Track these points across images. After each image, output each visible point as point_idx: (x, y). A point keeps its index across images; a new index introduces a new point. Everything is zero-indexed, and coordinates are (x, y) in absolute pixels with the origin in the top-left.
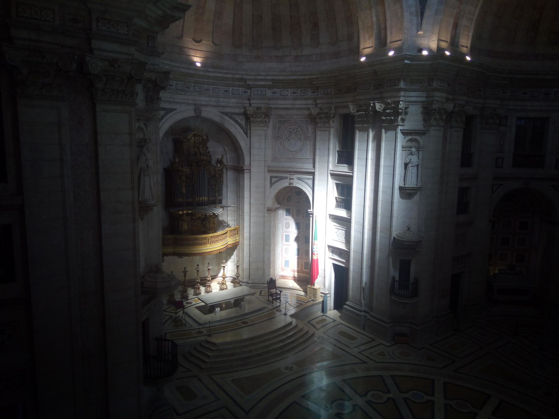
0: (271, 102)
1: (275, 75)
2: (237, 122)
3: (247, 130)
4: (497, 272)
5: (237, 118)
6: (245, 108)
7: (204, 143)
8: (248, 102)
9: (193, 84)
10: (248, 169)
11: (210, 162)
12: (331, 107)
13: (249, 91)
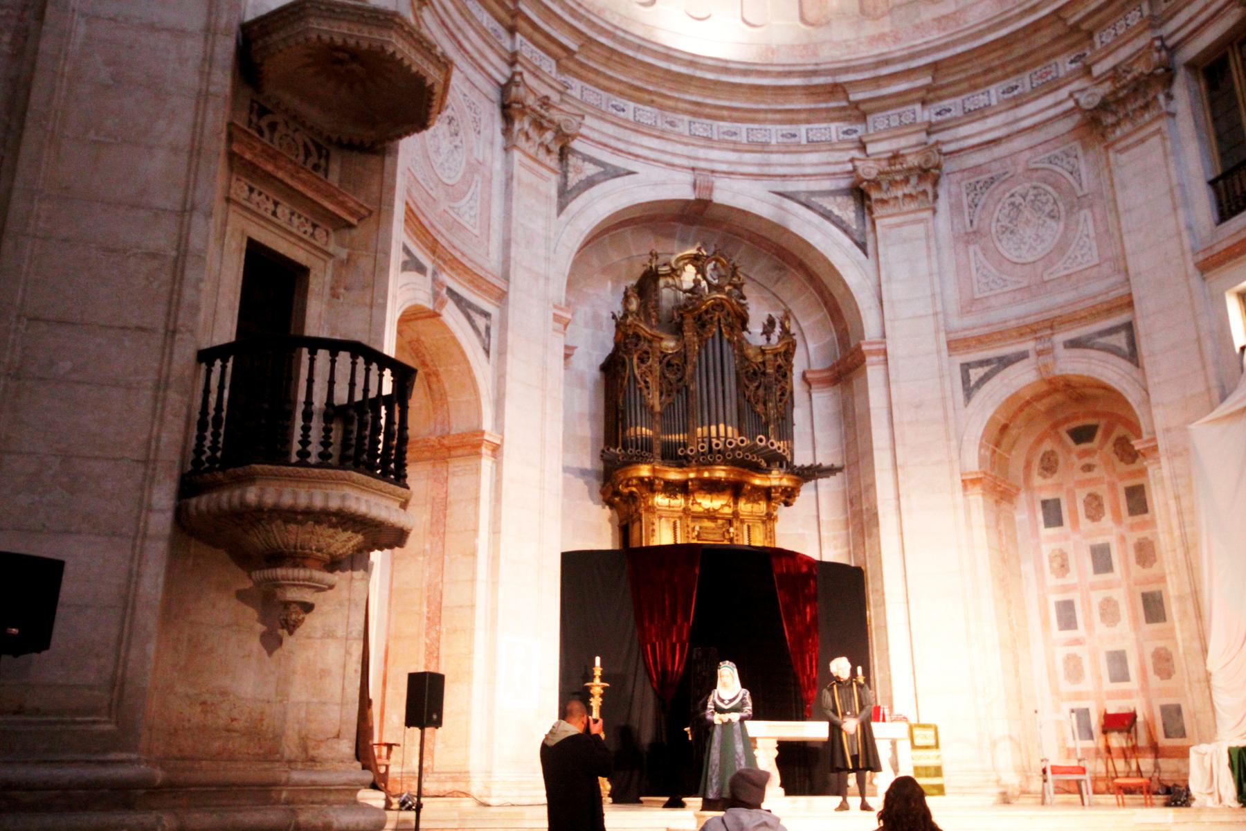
0: (934, 138)
2: (827, 215)
3: (863, 234)
9: (687, 118)
10: (877, 353)
11: (743, 321)
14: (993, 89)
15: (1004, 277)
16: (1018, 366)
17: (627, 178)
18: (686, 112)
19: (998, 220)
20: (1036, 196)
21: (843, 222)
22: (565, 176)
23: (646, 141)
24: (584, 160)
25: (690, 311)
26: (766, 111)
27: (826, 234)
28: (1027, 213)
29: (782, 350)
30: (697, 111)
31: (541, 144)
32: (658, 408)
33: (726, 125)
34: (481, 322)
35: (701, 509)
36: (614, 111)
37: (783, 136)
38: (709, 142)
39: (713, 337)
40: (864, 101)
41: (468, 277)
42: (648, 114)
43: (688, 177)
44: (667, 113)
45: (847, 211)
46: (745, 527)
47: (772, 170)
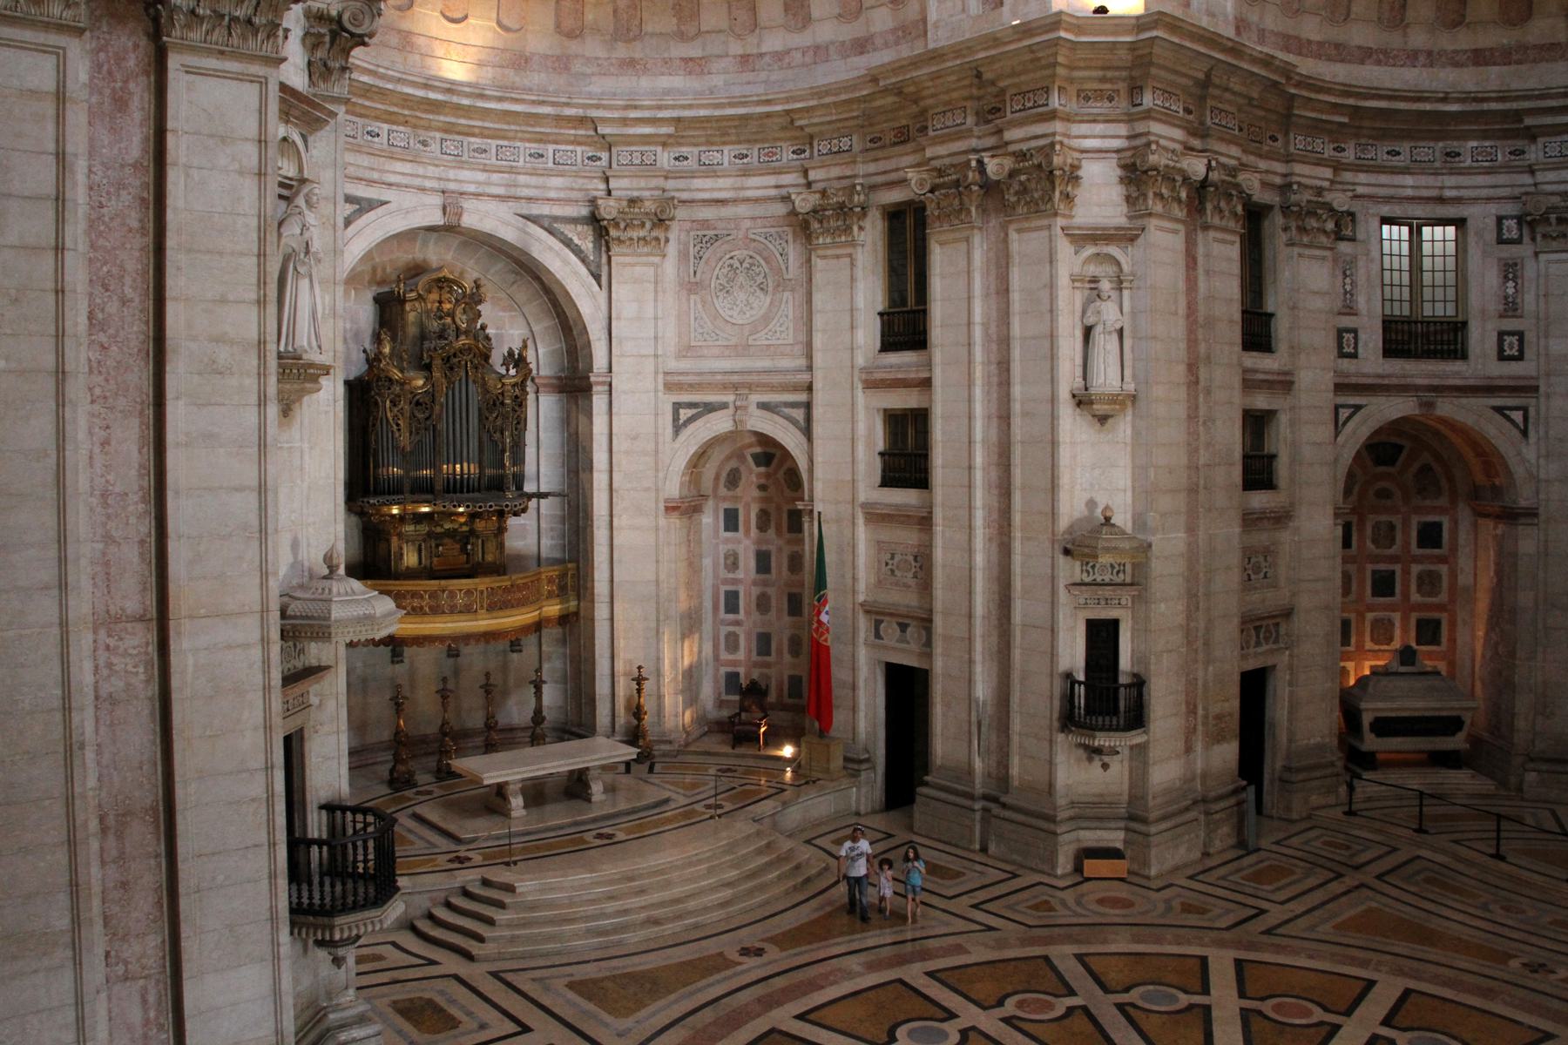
0: (671, 184)
1: (683, 107)
2: (568, 243)
3: (599, 266)
4: (1367, 672)
6: (593, 202)
7: (473, 300)
8: (602, 186)
9: (438, 135)
12: (854, 186)
13: (604, 155)
14: (726, 149)
18: (438, 130)
23: (399, 166)
27: (566, 262)
28: (741, 278)
30: (448, 129)
33: (476, 142)
42: (401, 134)
44: (420, 132)
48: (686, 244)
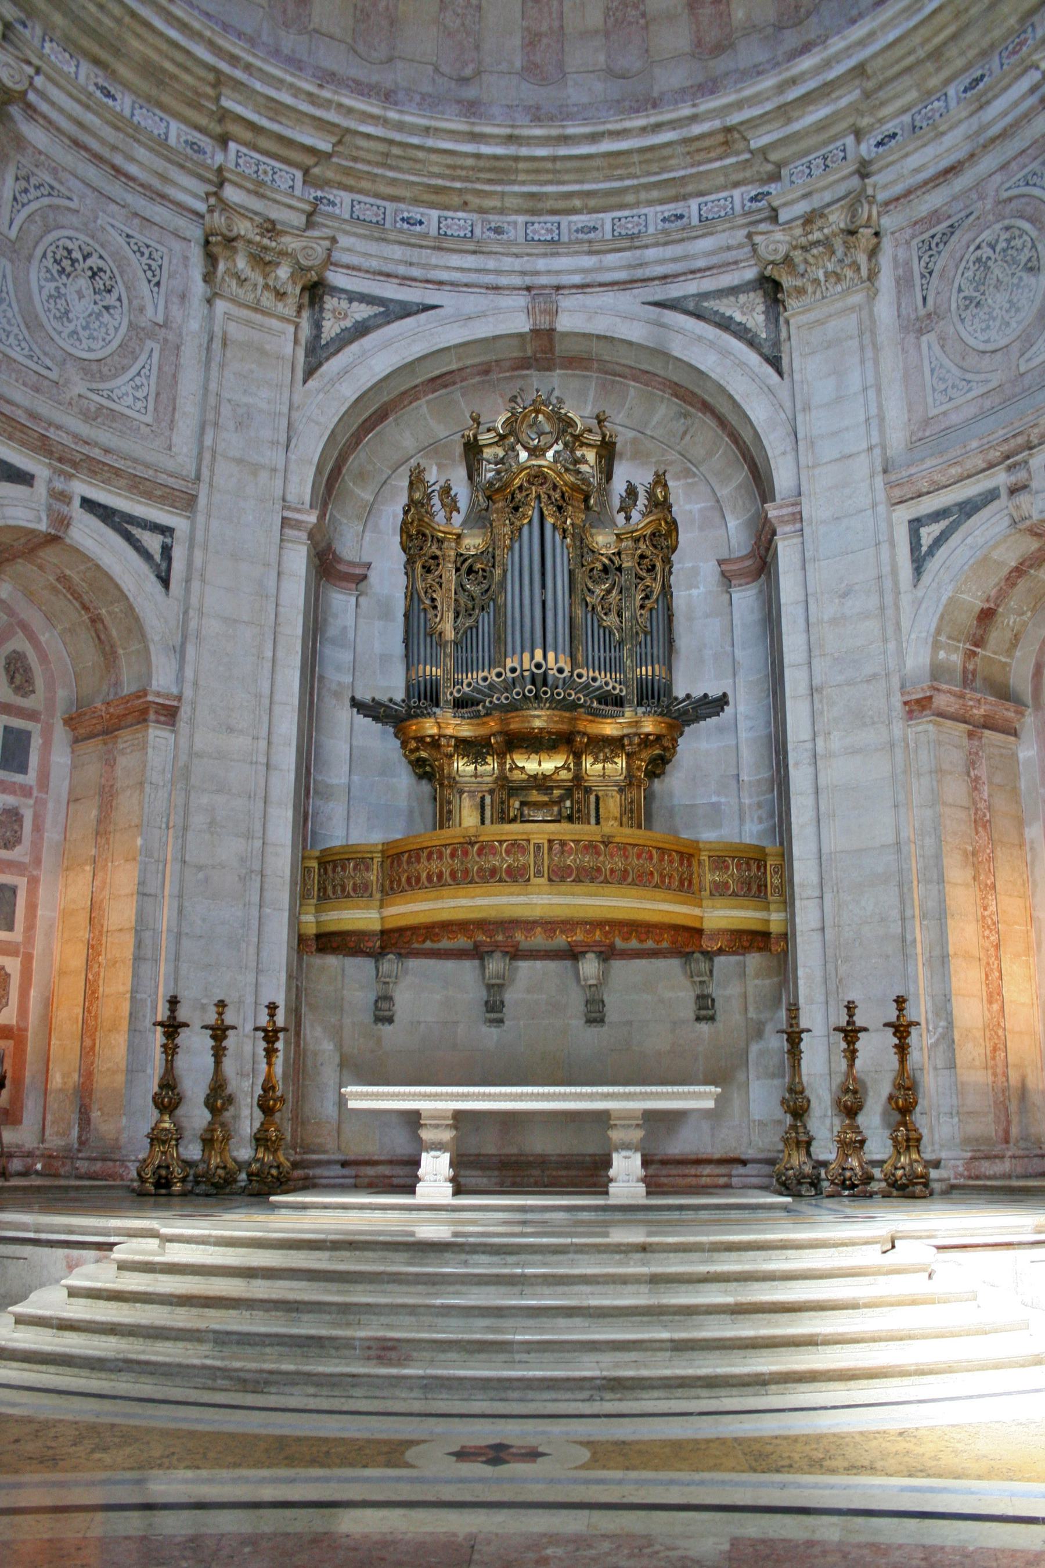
2: (725, 324)
3: (777, 344)
5: (728, 308)
9: (521, 219)
15: (969, 376)
16: (985, 513)
17: (423, 316)
18: (518, 212)
19: (960, 290)
20: (1008, 241)
21: (747, 330)
22: (317, 326)
23: (455, 260)
24: (351, 301)
25: (498, 490)
26: (636, 189)
27: (725, 353)
28: (997, 272)
29: (649, 532)
30: (534, 205)
31: (266, 286)
32: (450, 635)
34: (153, 542)
35: (524, 776)
36: (405, 226)
37: (664, 220)
38: (553, 245)
39: (530, 523)
40: (773, 145)
41: (123, 482)
42: (460, 221)
43: (521, 300)
44: (491, 217)
45: (751, 313)
46: (592, 798)
47: (648, 272)
48: (908, 263)
